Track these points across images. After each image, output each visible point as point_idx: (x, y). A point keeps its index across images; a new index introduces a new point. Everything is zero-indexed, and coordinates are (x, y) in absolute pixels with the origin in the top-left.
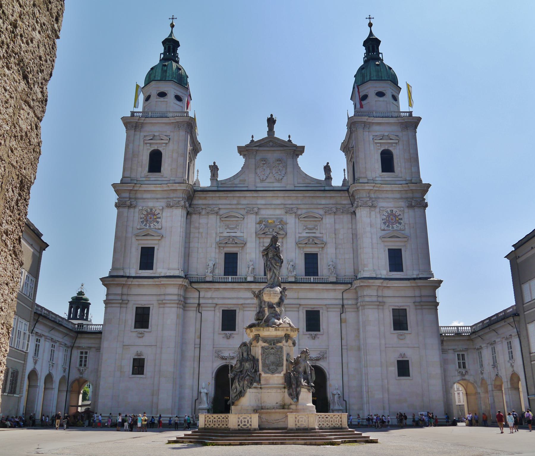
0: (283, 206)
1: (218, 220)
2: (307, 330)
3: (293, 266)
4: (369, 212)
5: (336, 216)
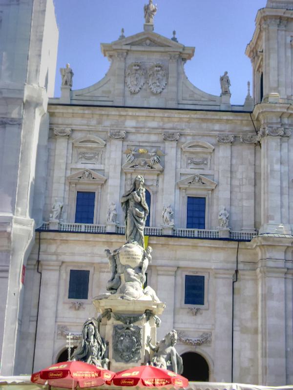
0: (160, 130)
1: (70, 145)
2: (187, 302)
3: (170, 213)
4: (279, 144)
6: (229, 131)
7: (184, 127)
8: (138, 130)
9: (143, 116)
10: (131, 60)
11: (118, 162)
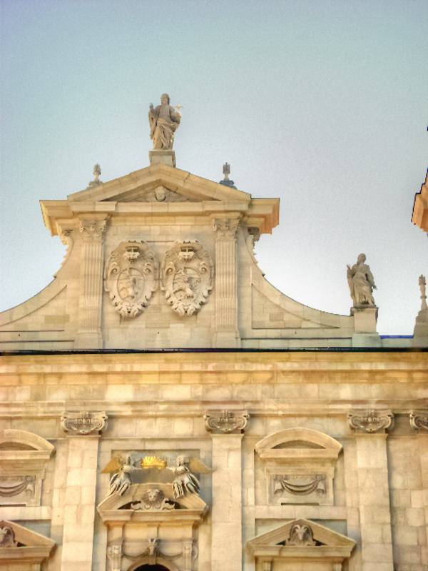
0: (198, 407)
5: (396, 445)
6: (379, 402)
7: (259, 395)
8: (139, 409)
9: (149, 373)
10: (118, 237)
11: (88, 496)
